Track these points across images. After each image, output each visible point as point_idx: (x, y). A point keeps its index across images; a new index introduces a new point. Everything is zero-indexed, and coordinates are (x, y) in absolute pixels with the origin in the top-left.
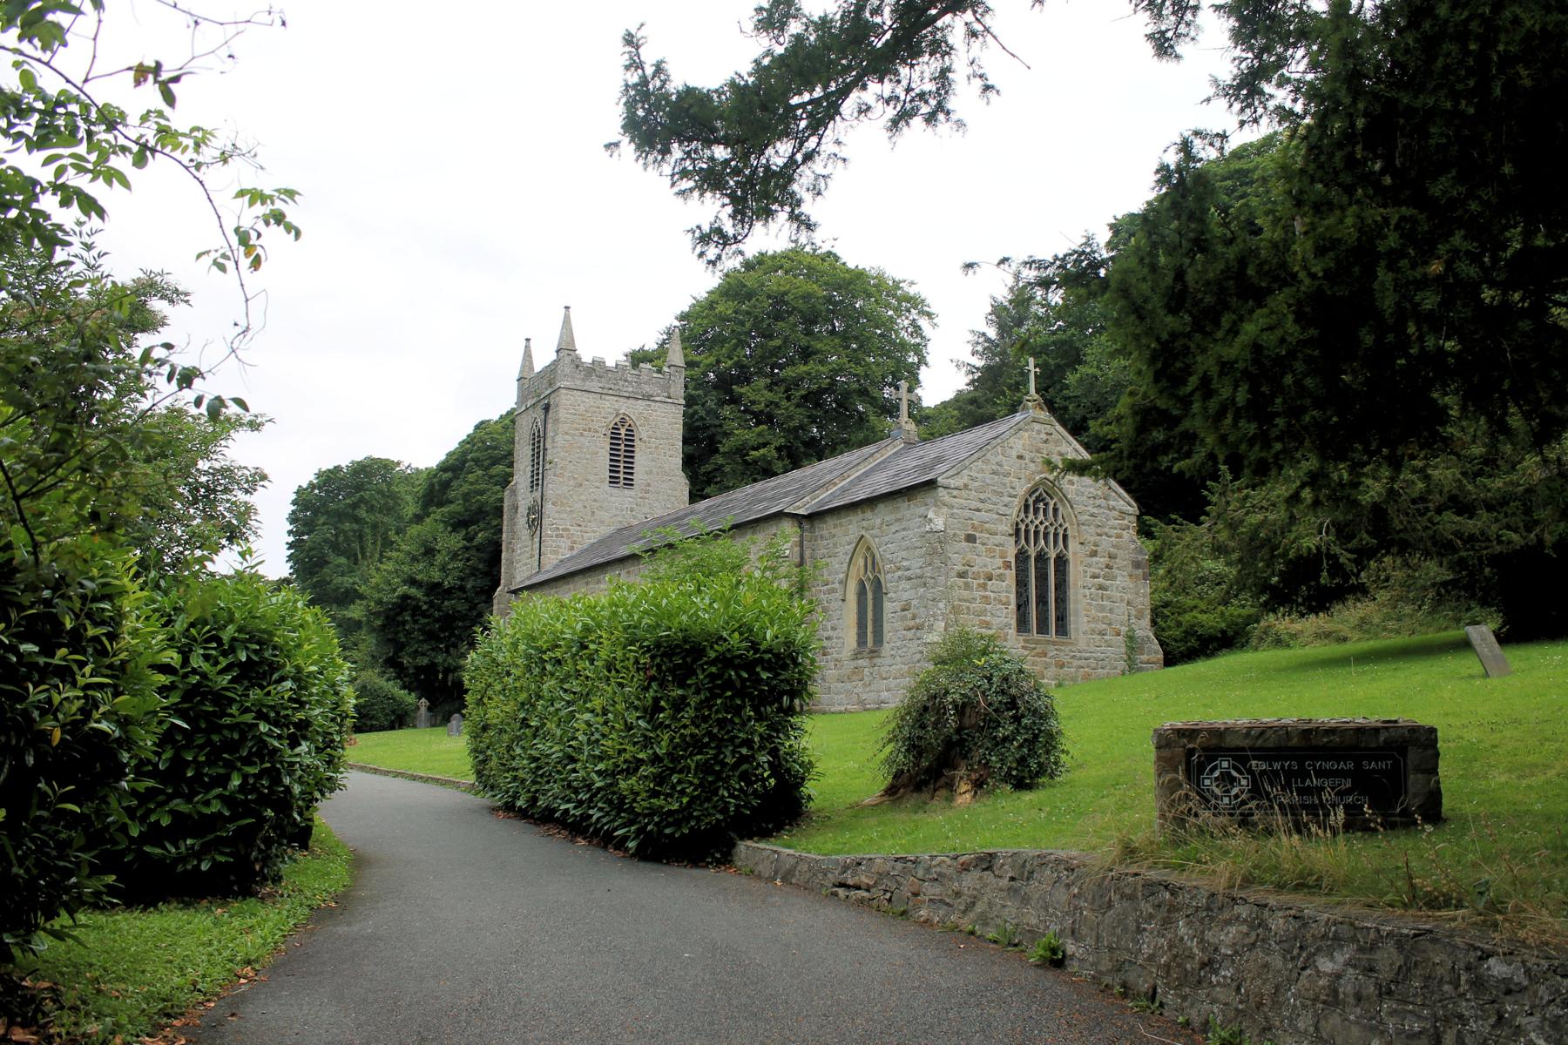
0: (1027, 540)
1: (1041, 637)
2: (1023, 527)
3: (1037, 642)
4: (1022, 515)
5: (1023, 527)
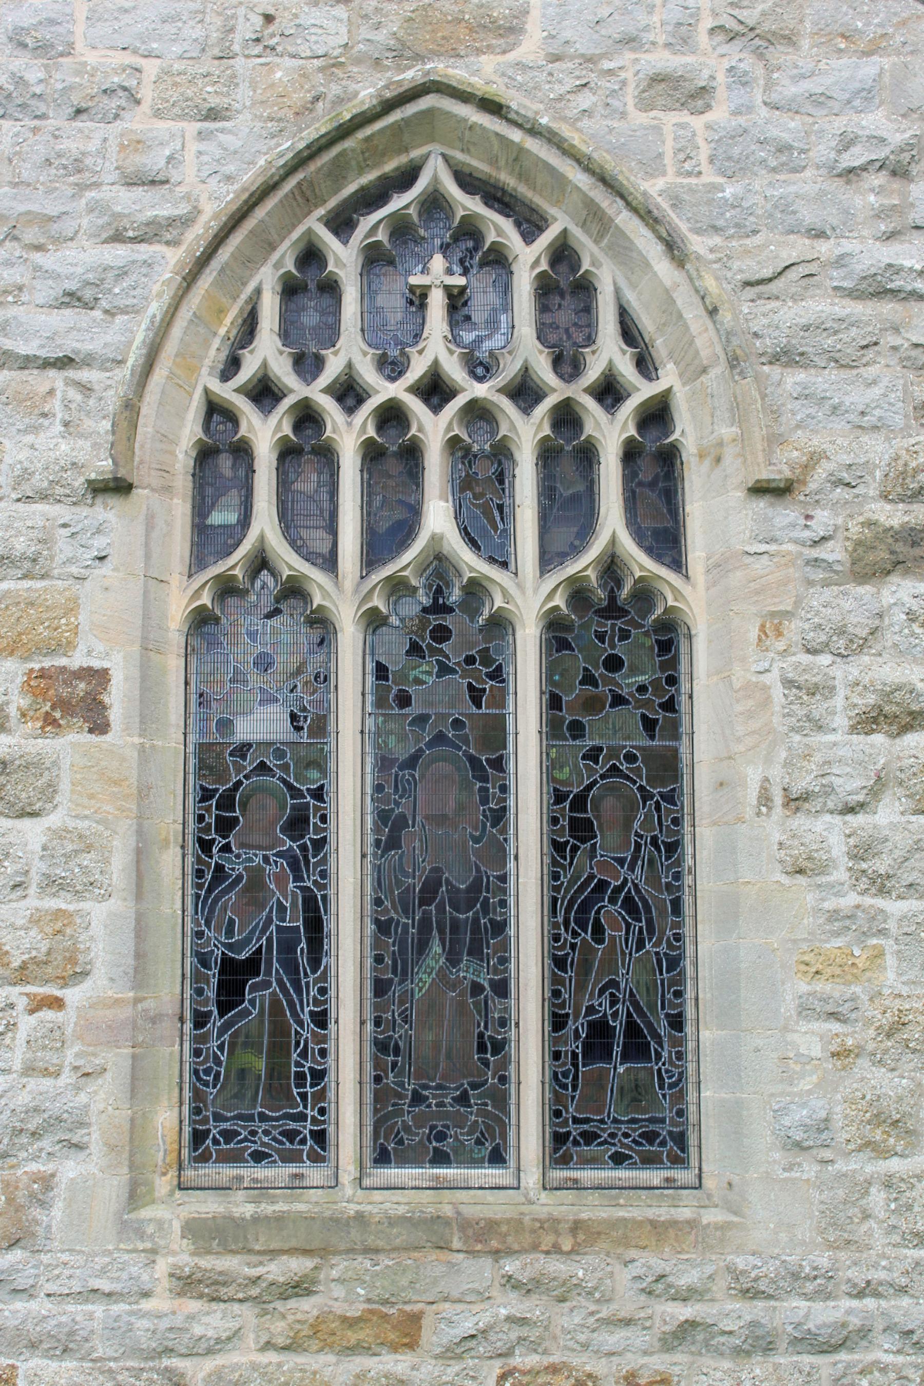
0: (310, 517)
1: (409, 1187)
2: (264, 432)
3: (328, 1239)
4: (268, 353)
5: (264, 432)
